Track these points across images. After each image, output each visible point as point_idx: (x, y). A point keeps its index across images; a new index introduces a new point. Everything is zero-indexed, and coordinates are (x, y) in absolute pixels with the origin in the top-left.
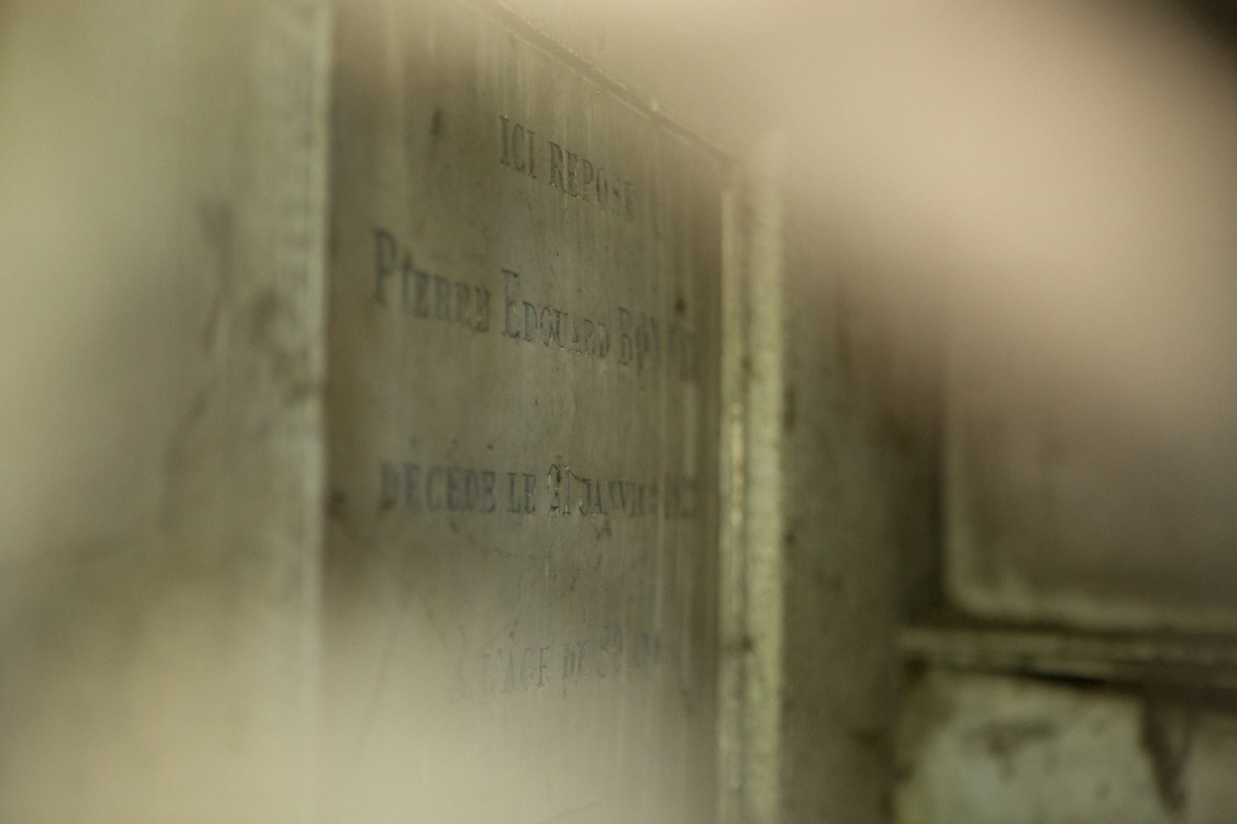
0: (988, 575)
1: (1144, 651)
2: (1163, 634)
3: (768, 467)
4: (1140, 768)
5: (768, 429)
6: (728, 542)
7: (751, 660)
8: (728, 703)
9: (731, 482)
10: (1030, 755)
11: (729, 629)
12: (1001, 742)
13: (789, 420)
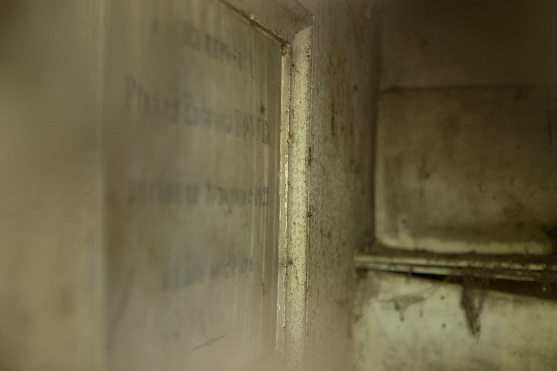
0: (394, 231)
1: (463, 264)
2: (472, 256)
3: (300, 182)
4: (461, 316)
5: (300, 165)
6: (283, 233)
7: (292, 269)
8: (281, 289)
9: (283, 189)
10: (412, 310)
11: (282, 255)
12: (399, 305)
13: (309, 161)
